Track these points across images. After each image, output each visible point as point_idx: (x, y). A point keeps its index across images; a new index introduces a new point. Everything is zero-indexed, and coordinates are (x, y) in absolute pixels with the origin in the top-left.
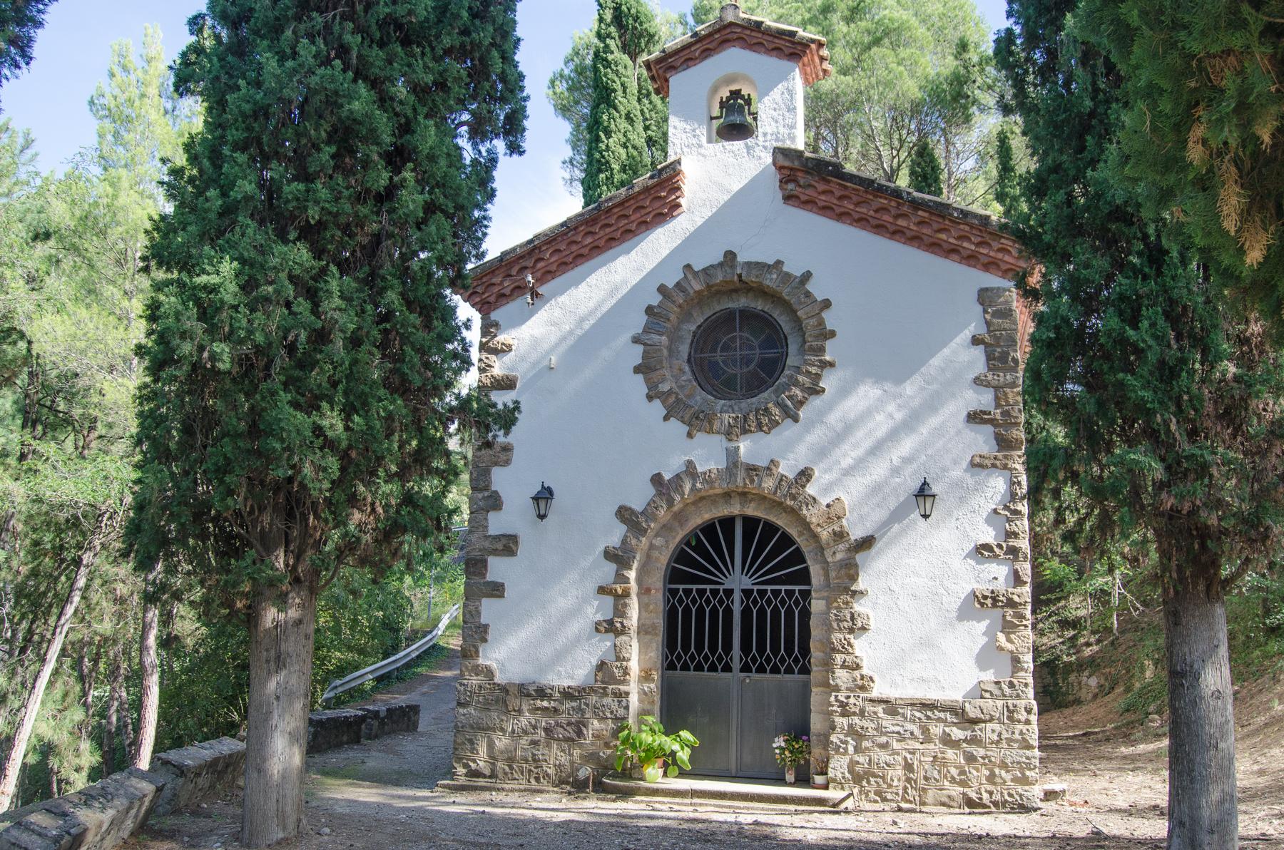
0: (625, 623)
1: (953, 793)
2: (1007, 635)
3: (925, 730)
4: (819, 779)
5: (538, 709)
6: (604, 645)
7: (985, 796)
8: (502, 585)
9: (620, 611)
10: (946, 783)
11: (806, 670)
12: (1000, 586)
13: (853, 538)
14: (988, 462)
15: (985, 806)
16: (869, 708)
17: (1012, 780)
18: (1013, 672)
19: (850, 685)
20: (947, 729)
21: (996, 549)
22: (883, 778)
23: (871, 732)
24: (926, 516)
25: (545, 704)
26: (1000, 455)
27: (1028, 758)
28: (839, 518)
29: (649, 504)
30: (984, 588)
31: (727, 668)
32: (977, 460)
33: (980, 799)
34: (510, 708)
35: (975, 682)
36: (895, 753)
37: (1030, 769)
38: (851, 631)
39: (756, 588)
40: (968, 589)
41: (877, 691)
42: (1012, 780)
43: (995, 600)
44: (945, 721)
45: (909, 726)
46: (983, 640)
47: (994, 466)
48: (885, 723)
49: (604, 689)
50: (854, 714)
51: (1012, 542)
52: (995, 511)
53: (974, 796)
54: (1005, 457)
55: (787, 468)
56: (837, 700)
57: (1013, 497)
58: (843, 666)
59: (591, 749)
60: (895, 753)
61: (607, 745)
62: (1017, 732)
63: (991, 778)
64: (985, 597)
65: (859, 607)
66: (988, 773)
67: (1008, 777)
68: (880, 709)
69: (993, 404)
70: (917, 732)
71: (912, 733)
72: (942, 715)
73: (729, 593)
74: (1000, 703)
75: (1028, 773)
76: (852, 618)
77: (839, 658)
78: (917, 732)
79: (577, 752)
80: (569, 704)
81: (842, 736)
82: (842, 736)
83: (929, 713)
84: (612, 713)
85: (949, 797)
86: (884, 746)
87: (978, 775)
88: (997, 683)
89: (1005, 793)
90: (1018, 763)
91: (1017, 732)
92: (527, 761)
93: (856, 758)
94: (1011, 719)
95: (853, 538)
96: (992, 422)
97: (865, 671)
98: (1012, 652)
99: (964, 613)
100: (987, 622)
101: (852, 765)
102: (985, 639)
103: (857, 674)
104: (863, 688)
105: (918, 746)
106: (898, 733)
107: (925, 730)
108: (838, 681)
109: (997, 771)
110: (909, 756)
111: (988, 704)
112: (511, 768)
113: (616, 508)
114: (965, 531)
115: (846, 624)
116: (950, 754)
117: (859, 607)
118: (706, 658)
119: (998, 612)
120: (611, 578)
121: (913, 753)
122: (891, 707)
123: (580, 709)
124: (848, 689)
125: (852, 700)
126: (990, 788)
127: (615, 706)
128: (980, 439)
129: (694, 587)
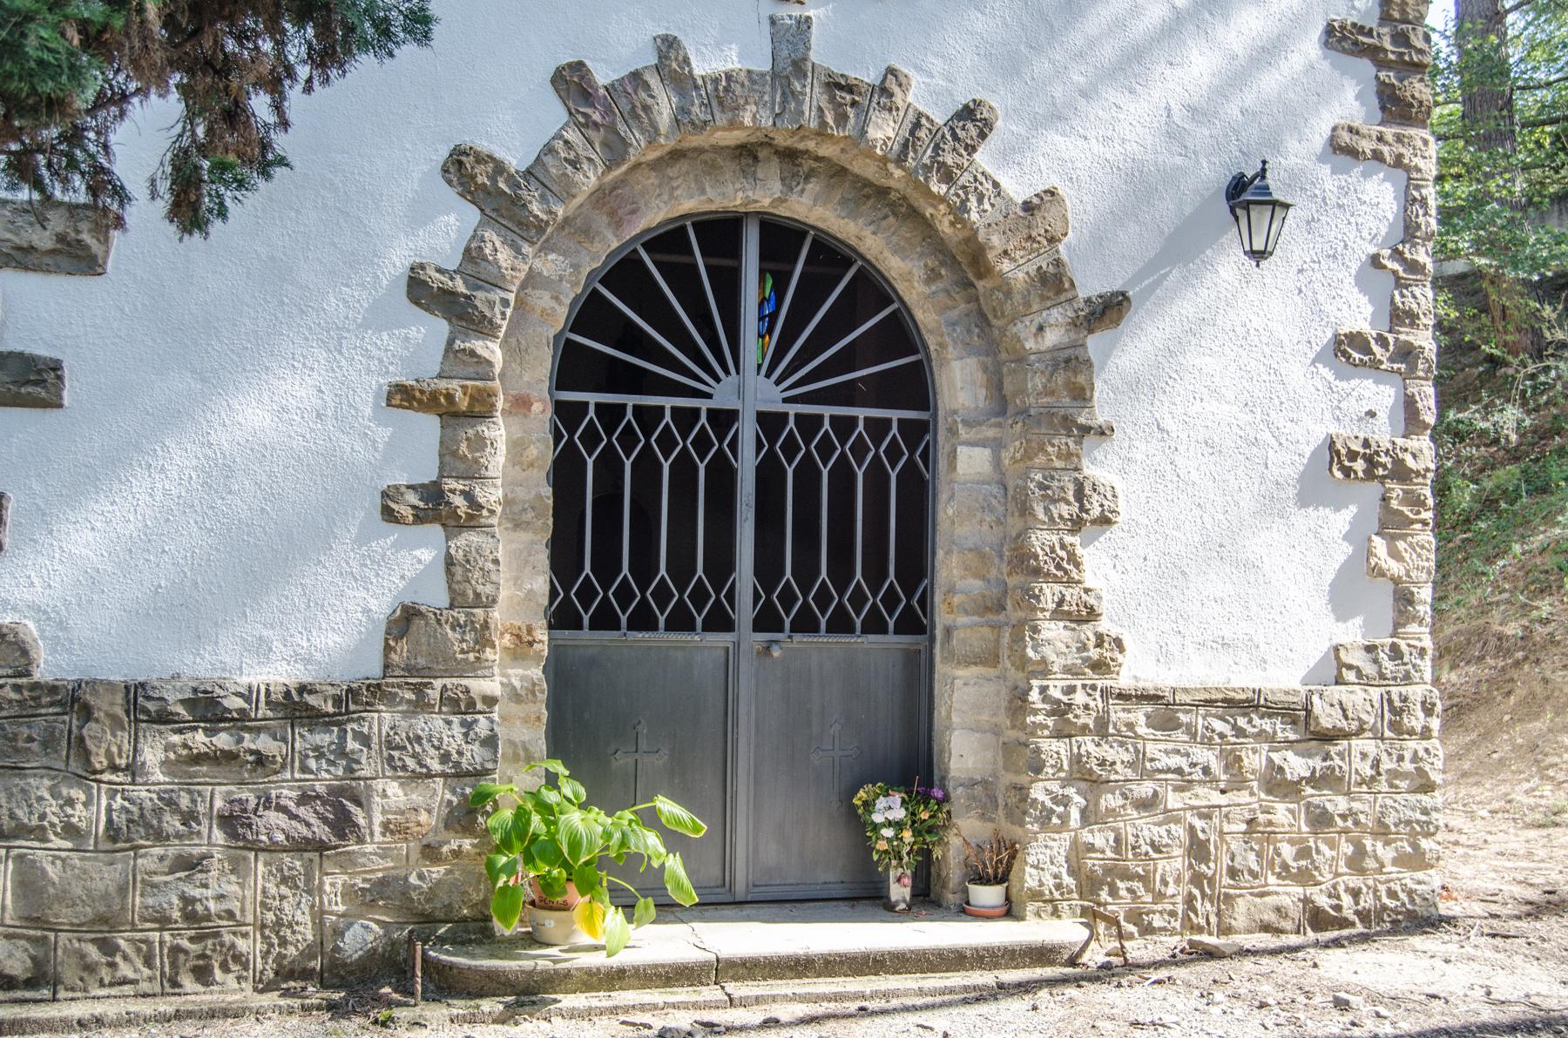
0: (481, 496)
1: (1286, 901)
2: (1391, 539)
3: (1233, 762)
4: (987, 896)
5: (198, 759)
6: (412, 563)
7: (1347, 900)
8: (56, 367)
9: (459, 462)
10: (1272, 879)
11: (915, 623)
12: (1383, 433)
13: (1082, 294)
14: (1366, 146)
15: (1345, 923)
16: (1118, 714)
17: (1395, 862)
18: (1397, 625)
19: (1073, 659)
20: (1275, 757)
21: (1376, 348)
22: (1145, 879)
23: (1123, 772)
24: (1259, 255)
25: (223, 741)
26: (1389, 132)
27: (1425, 812)
28: (1052, 240)
29: (549, 149)
30: (1349, 433)
31: (720, 621)
32: (1345, 137)
33: (1338, 908)
34: (99, 761)
35: (1325, 646)
36: (1171, 817)
37: (1428, 835)
38: (1077, 525)
39: (793, 409)
40: (1319, 434)
41: (1134, 671)
42: (1395, 862)
43: (1371, 462)
44: (1270, 738)
45: (1204, 755)
46: (1342, 552)
47: (1377, 156)
48: (1151, 749)
49: (419, 689)
50: (1084, 730)
51: (1407, 335)
52: (1375, 261)
53: (1323, 902)
54: (1399, 139)
55: (929, 94)
56: (1046, 698)
57: (1410, 231)
58: (1059, 613)
59: (380, 867)
60: (1171, 817)
61: (431, 852)
62: (1408, 755)
63: (1356, 862)
64: (1353, 456)
65: (1099, 467)
66: (1348, 849)
67: (1386, 854)
68: (1139, 716)
69: (1377, 13)
70: (1216, 767)
71: (1206, 770)
72: (1266, 724)
73: (724, 420)
74: (1375, 693)
75: (1425, 844)
76: (1080, 494)
77: (1049, 593)
78: (1216, 767)
79: (333, 883)
80: (307, 739)
81: (1055, 787)
82: (1055, 787)
83: (1242, 722)
84: (445, 758)
85: (1278, 909)
86: (1146, 805)
87: (1331, 854)
88: (1370, 649)
89: (1382, 888)
90: (1408, 823)
91: (1408, 755)
92: (163, 922)
93: (1086, 836)
94: (1396, 727)
95: (1082, 294)
96: (1374, 53)
97: (1104, 626)
98: (1396, 581)
99: (1310, 493)
100: (1353, 509)
101: (1079, 851)
102: (1349, 549)
103: (1088, 631)
104: (1099, 666)
105: (1217, 798)
106: (1179, 771)
107: (1233, 762)
108: (1047, 651)
109: (1368, 843)
110: (1199, 824)
111: (1359, 699)
112: (108, 947)
113: (443, 153)
114: (1316, 302)
115: (1064, 510)
116: (1282, 812)
117: (1099, 467)
118: (624, 595)
119: (1374, 488)
120: (432, 362)
121: (1208, 817)
122: (1164, 709)
123: (342, 752)
124: (1067, 670)
125: (1080, 698)
126: (1355, 881)
127: (453, 736)
128: (1350, 91)
129: (631, 400)
